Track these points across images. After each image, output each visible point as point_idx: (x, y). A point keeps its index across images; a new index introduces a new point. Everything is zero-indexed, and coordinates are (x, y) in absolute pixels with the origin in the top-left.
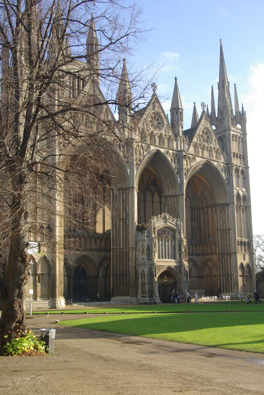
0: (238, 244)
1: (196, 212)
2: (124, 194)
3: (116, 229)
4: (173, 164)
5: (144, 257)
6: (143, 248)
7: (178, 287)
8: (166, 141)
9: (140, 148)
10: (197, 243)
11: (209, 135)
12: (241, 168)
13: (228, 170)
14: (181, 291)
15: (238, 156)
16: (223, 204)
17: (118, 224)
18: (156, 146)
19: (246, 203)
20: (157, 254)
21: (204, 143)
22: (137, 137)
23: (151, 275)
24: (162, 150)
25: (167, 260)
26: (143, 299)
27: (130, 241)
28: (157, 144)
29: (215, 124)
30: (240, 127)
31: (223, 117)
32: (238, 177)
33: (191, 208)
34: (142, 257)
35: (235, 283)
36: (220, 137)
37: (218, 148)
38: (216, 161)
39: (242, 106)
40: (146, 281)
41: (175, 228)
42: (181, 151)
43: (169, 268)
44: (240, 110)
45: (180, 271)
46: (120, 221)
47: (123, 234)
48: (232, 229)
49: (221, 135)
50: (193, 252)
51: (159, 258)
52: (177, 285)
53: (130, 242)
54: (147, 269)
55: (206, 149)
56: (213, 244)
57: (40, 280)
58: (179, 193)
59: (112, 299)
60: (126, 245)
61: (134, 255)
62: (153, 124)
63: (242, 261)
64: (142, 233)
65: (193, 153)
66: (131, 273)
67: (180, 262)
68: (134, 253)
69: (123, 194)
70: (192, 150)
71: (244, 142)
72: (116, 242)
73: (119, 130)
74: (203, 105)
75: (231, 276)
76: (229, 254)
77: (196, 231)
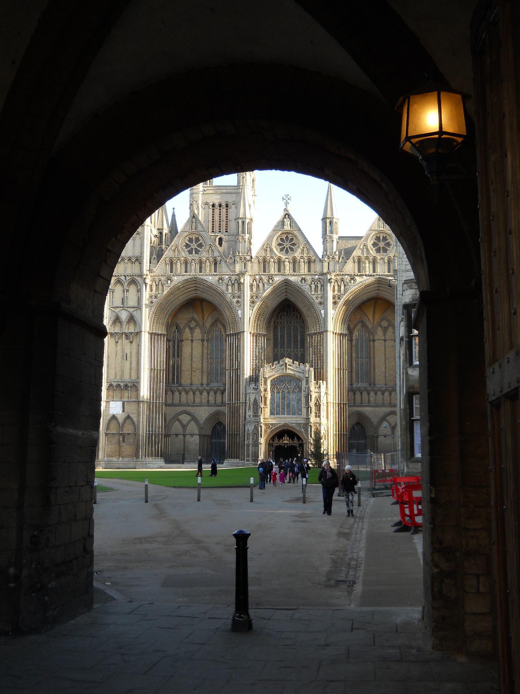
4: (313, 293)
11: (388, 241)
20: (268, 411)
23: (256, 434)
26: (247, 463)
34: (250, 413)
40: (251, 442)
41: (301, 375)
43: (285, 425)
45: (306, 430)
51: (272, 413)
54: (253, 427)
57: (125, 440)
58: (323, 330)
59: (225, 461)
67: (308, 419)
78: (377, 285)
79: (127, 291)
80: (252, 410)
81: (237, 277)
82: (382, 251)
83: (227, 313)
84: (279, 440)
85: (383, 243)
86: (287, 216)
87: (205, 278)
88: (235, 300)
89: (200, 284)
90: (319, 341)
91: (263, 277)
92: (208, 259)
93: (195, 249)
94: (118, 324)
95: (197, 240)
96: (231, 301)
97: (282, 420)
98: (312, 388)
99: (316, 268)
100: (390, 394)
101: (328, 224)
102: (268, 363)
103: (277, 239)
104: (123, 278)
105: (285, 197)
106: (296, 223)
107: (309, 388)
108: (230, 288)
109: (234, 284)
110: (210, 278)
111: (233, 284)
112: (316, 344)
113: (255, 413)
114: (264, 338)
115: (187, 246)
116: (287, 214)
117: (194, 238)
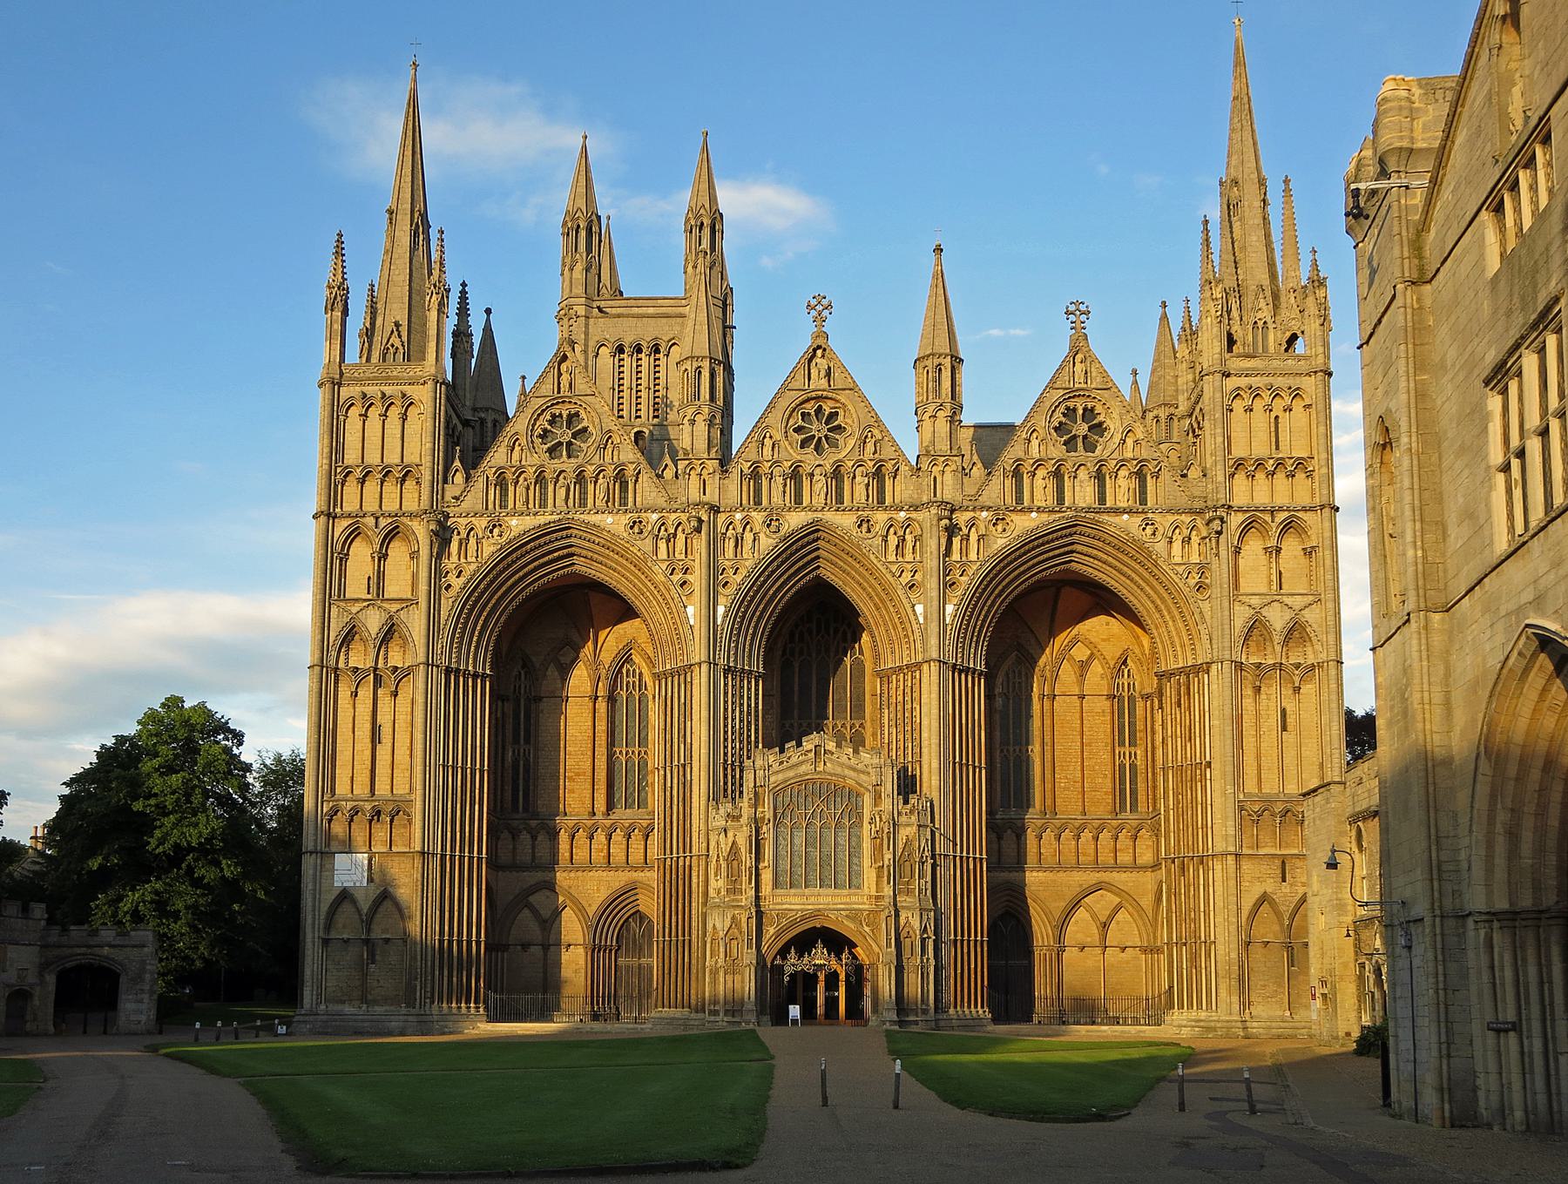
4: (892, 558)
13: (1205, 534)
16: (1181, 671)
28: (819, 501)
34: (718, 884)
38: (1130, 512)
40: (721, 962)
43: (816, 914)
54: (727, 924)
63: (1269, 886)
70: (998, 489)
79: (383, 556)
80: (724, 874)
81: (684, 517)
82: (1080, 444)
84: (801, 956)
85: (1086, 427)
90: (908, 690)
94: (356, 646)
97: (812, 899)
99: (900, 489)
102: (768, 745)
104: (370, 521)
108: (662, 545)
109: (675, 535)
110: (610, 520)
112: (900, 698)
114: (757, 685)
116: (819, 347)
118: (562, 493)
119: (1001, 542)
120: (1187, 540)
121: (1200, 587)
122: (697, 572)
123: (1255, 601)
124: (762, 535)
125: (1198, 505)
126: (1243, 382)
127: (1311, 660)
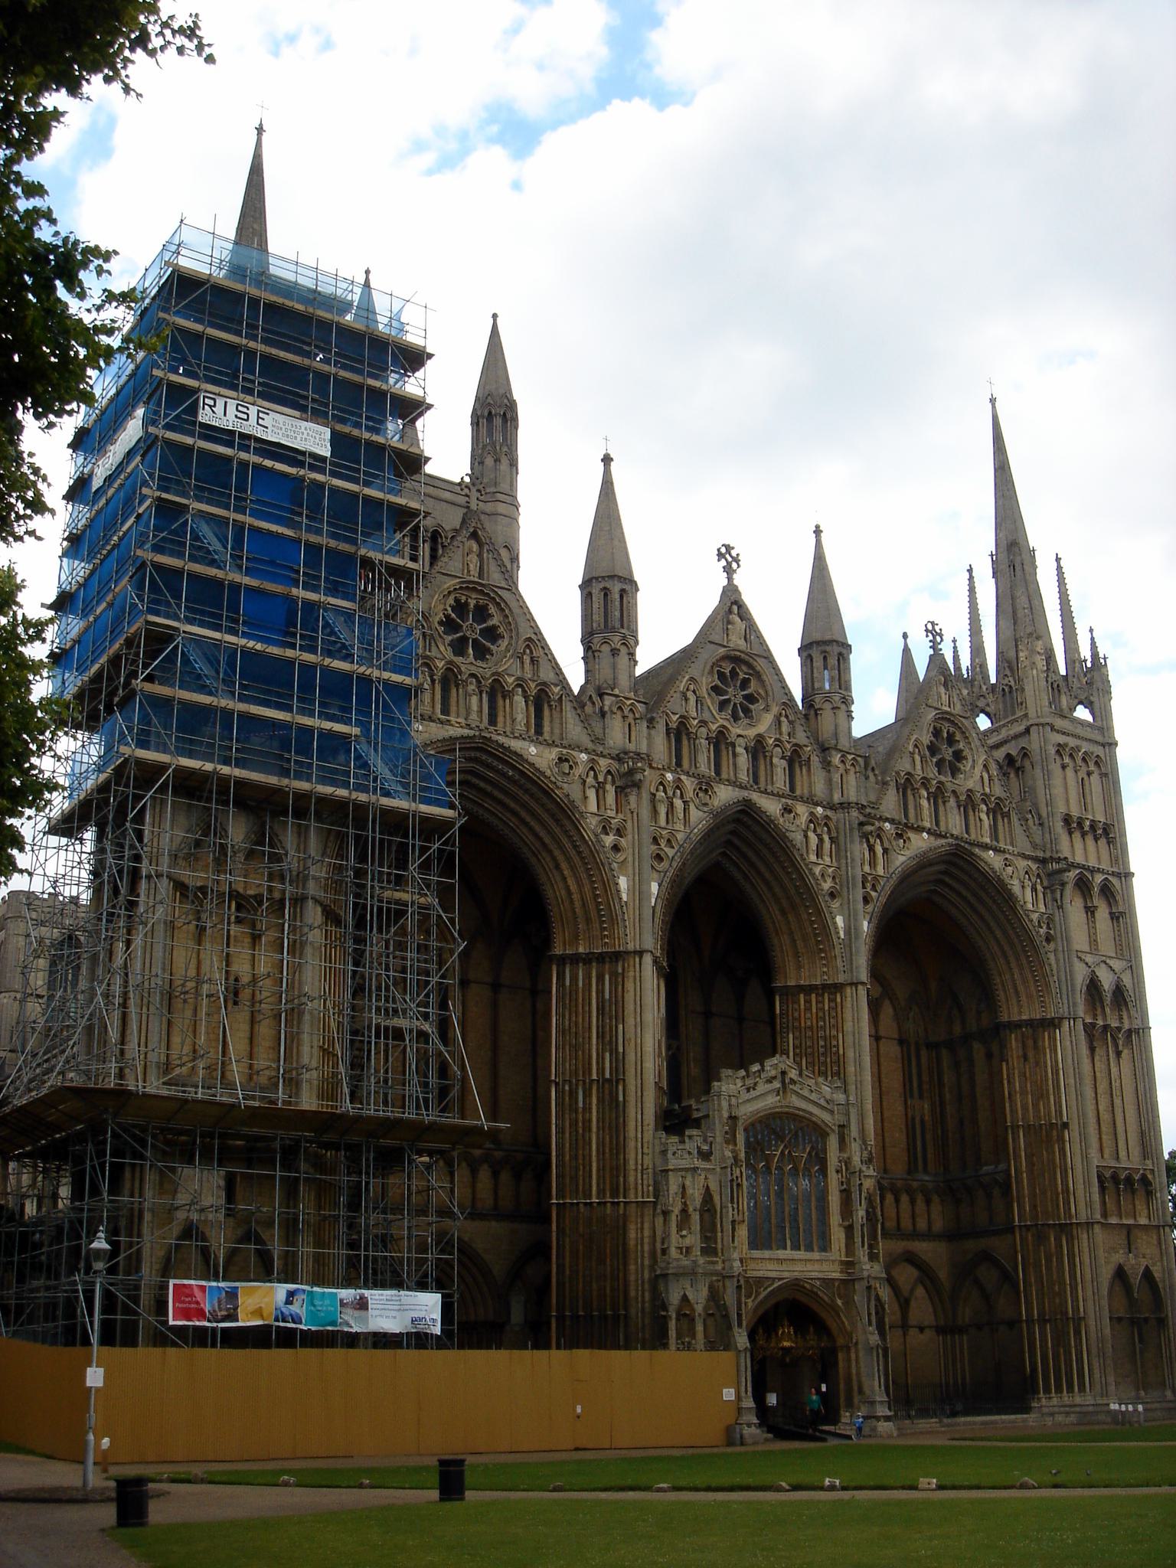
0: (1103, 1189)
1: (924, 1060)
2: (607, 977)
3: (574, 1124)
4: (813, 858)
5: (688, 1242)
6: (685, 1204)
7: (841, 1371)
8: (780, 764)
9: (670, 793)
10: (930, 1186)
11: (961, 746)
12: (1099, 878)
13: (1046, 884)
14: (856, 1388)
15: (1087, 828)
16: (1030, 1023)
17: (581, 1105)
18: (741, 787)
19: (1130, 1017)
20: (743, 1232)
21: (942, 778)
22: (660, 748)
24: (771, 807)
25: (788, 1253)
27: (632, 1173)
28: (743, 777)
29: (988, 709)
30: (1090, 718)
31: (1019, 680)
32: (1090, 911)
33: (901, 1042)
35: (1094, 1351)
36: (1008, 755)
37: (998, 798)
38: (996, 850)
39: (1092, 639)
41: (826, 1117)
42: (845, 806)
43: (796, 1284)
44: (1085, 652)
45: (849, 1302)
46: (591, 1089)
47: (601, 1144)
48: (1074, 1126)
49: (1013, 749)
50: (914, 1225)
51: (754, 1245)
52: (836, 1363)
53: (631, 1179)
54: (704, 1292)
55: (952, 802)
56: (996, 1192)
58: (841, 978)
60: (615, 1193)
61: (647, 1233)
62: (728, 701)
63: (1119, 1257)
64: (682, 1142)
65: (898, 816)
66: (633, 1311)
68: (646, 1225)
69: (600, 979)
70: (890, 804)
71: (1106, 775)
72: (574, 1179)
73: (585, 721)
74: (934, 633)
75: (1078, 1321)
76: (1066, 1229)
77: (929, 1136)
78: (942, 867)
83: (561, 888)
84: (768, 1339)
85: (950, 751)
86: (735, 608)
87: (516, 745)
88: (609, 840)
89: (489, 767)
91: (683, 777)
92: (521, 683)
93: (475, 641)
95: (482, 613)
96: (599, 841)
97: (784, 1267)
98: (856, 1160)
100: (897, 1201)
101: (832, 661)
103: (711, 672)
105: (723, 550)
106: (759, 636)
107: (848, 1162)
108: (592, 794)
110: (533, 750)
111: (600, 788)
113: (705, 1239)
115: (450, 625)
117: (472, 603)
118: (474, 700)
119: (902, 859)
120: (1034, 889)
121: (1049, 939)
122: (630, 837)
123: (1089, 959)
124: (692, 807)
125: (1040, 854)
126: (1062, 739)
127: (1126, 1026)
